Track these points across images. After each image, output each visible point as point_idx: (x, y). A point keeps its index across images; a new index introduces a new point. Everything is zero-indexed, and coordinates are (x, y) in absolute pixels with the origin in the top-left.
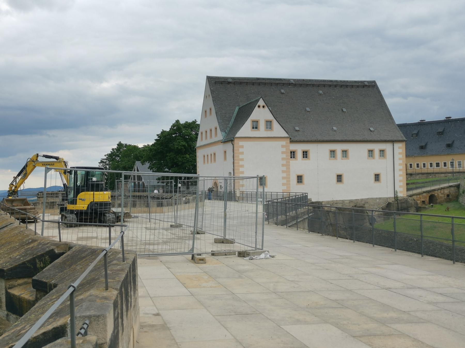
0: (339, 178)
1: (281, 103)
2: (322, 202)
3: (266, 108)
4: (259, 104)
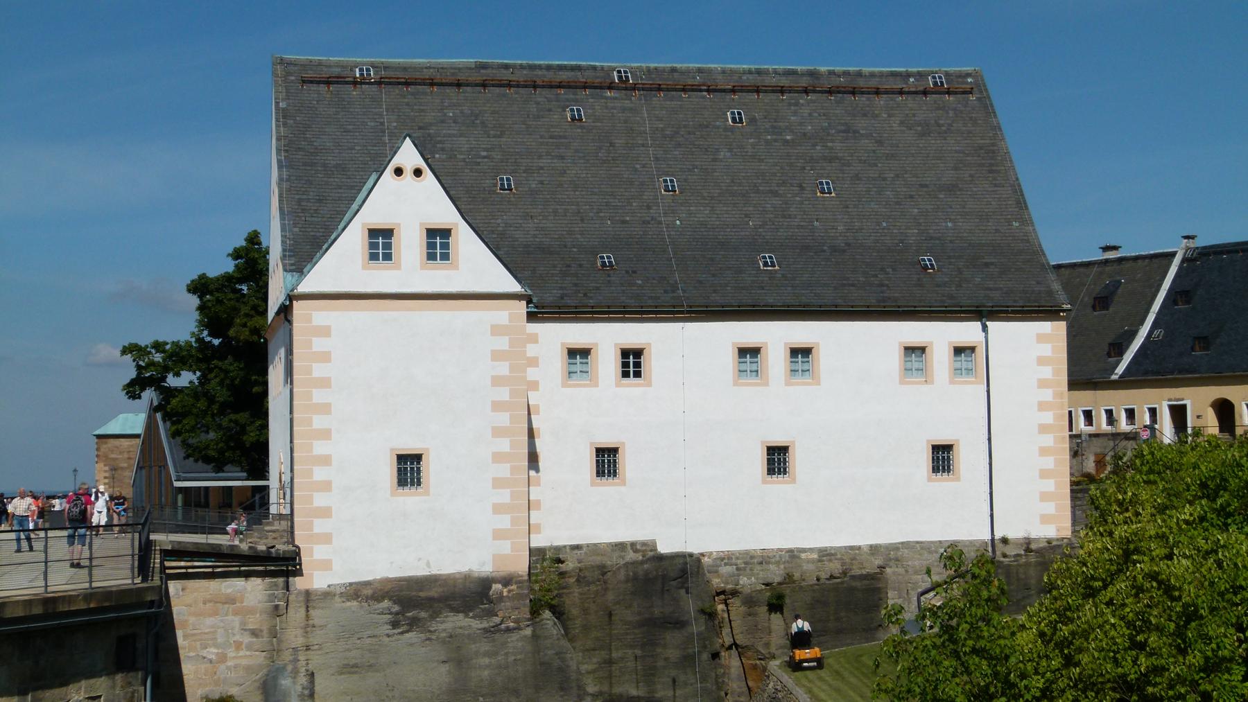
0: (777, 459)
1: (562, 158)
2: (703, 555)
3: (428, 175)
4: (397, 161)
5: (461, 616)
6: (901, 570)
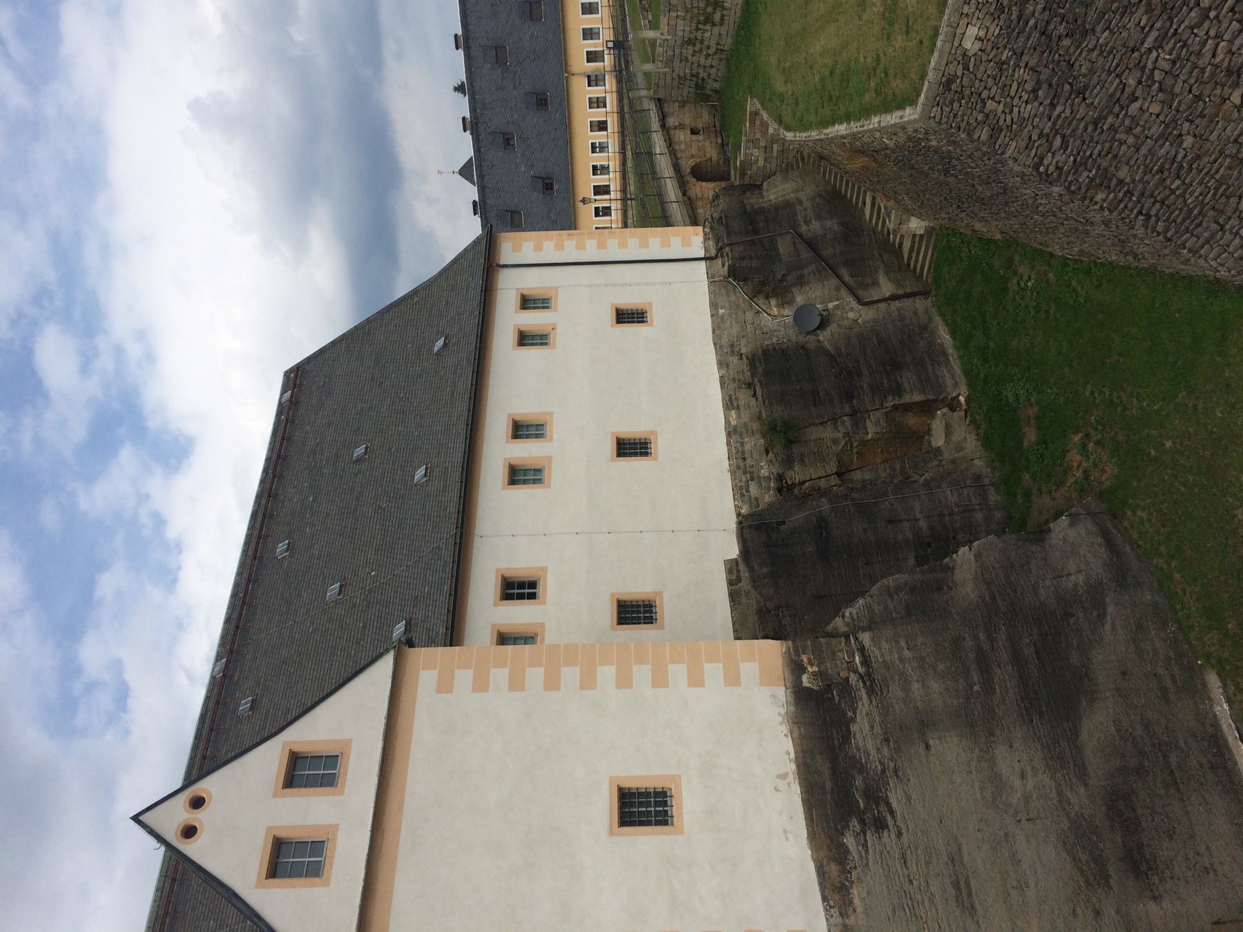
0: (631, 448)
2: (739, 515)
5: (854, 728)
6: (743, 342)
